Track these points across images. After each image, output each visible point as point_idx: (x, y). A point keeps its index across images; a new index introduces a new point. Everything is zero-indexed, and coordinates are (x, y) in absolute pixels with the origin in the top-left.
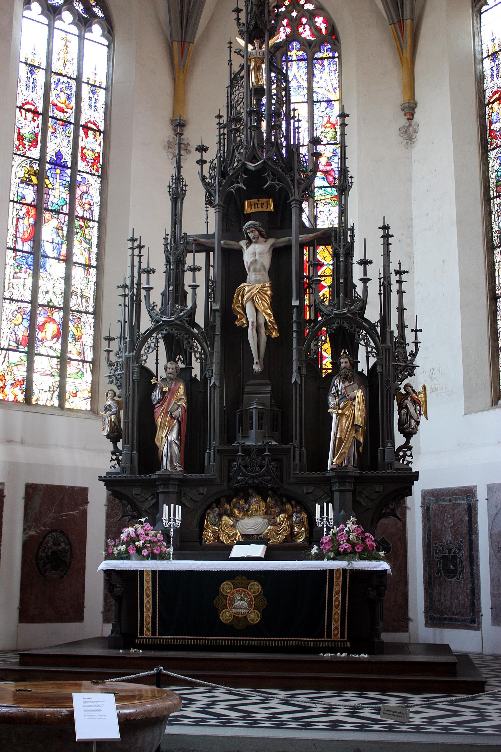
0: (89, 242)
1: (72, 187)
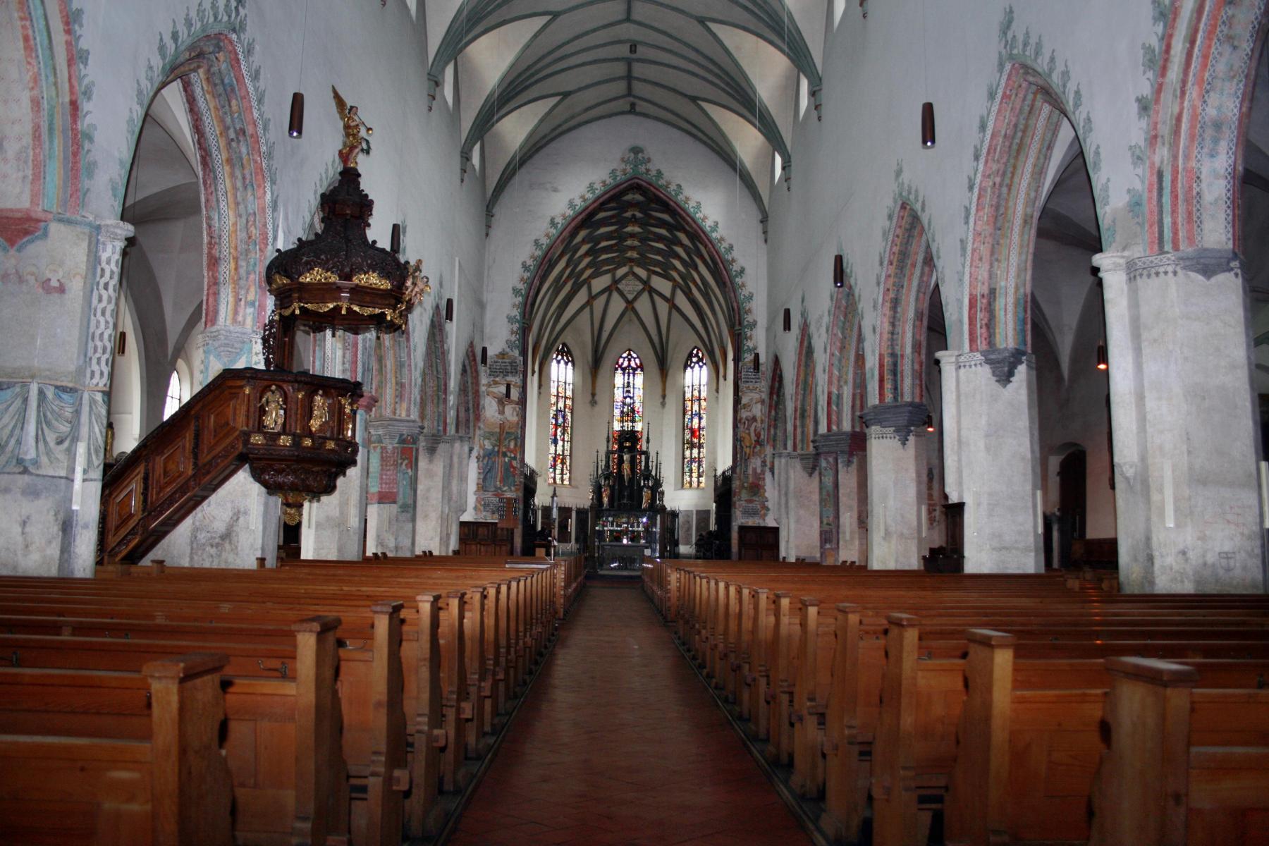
1: (564, 417)
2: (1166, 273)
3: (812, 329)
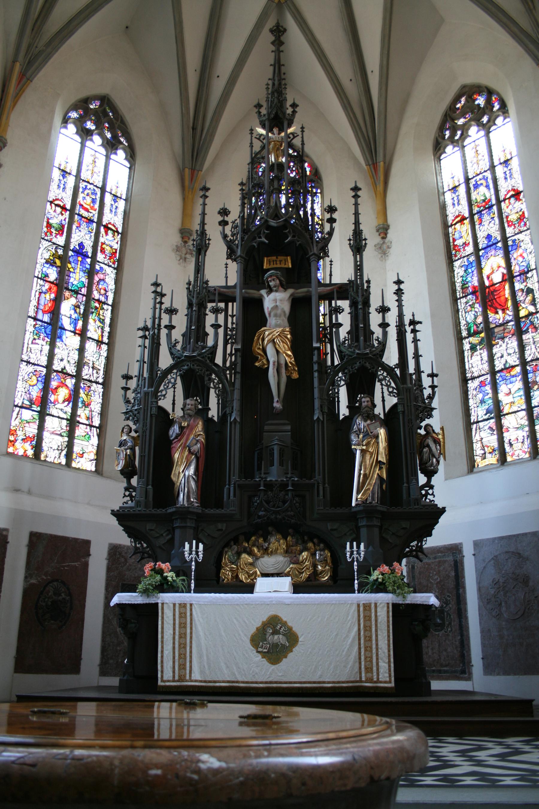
0: (102, 321)
1: (91, 273)
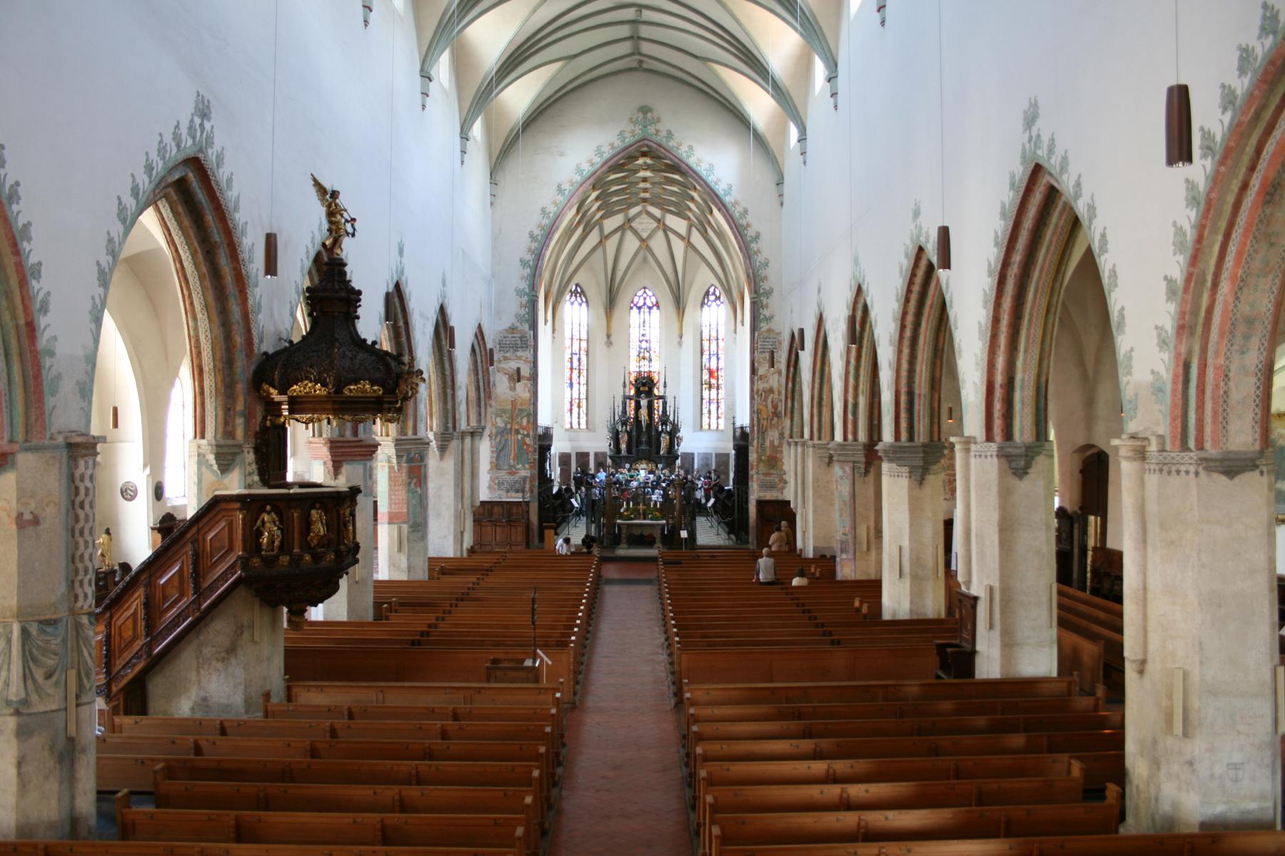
1: (579, 360)
2: (1187, 472)
3: (829, 326)
